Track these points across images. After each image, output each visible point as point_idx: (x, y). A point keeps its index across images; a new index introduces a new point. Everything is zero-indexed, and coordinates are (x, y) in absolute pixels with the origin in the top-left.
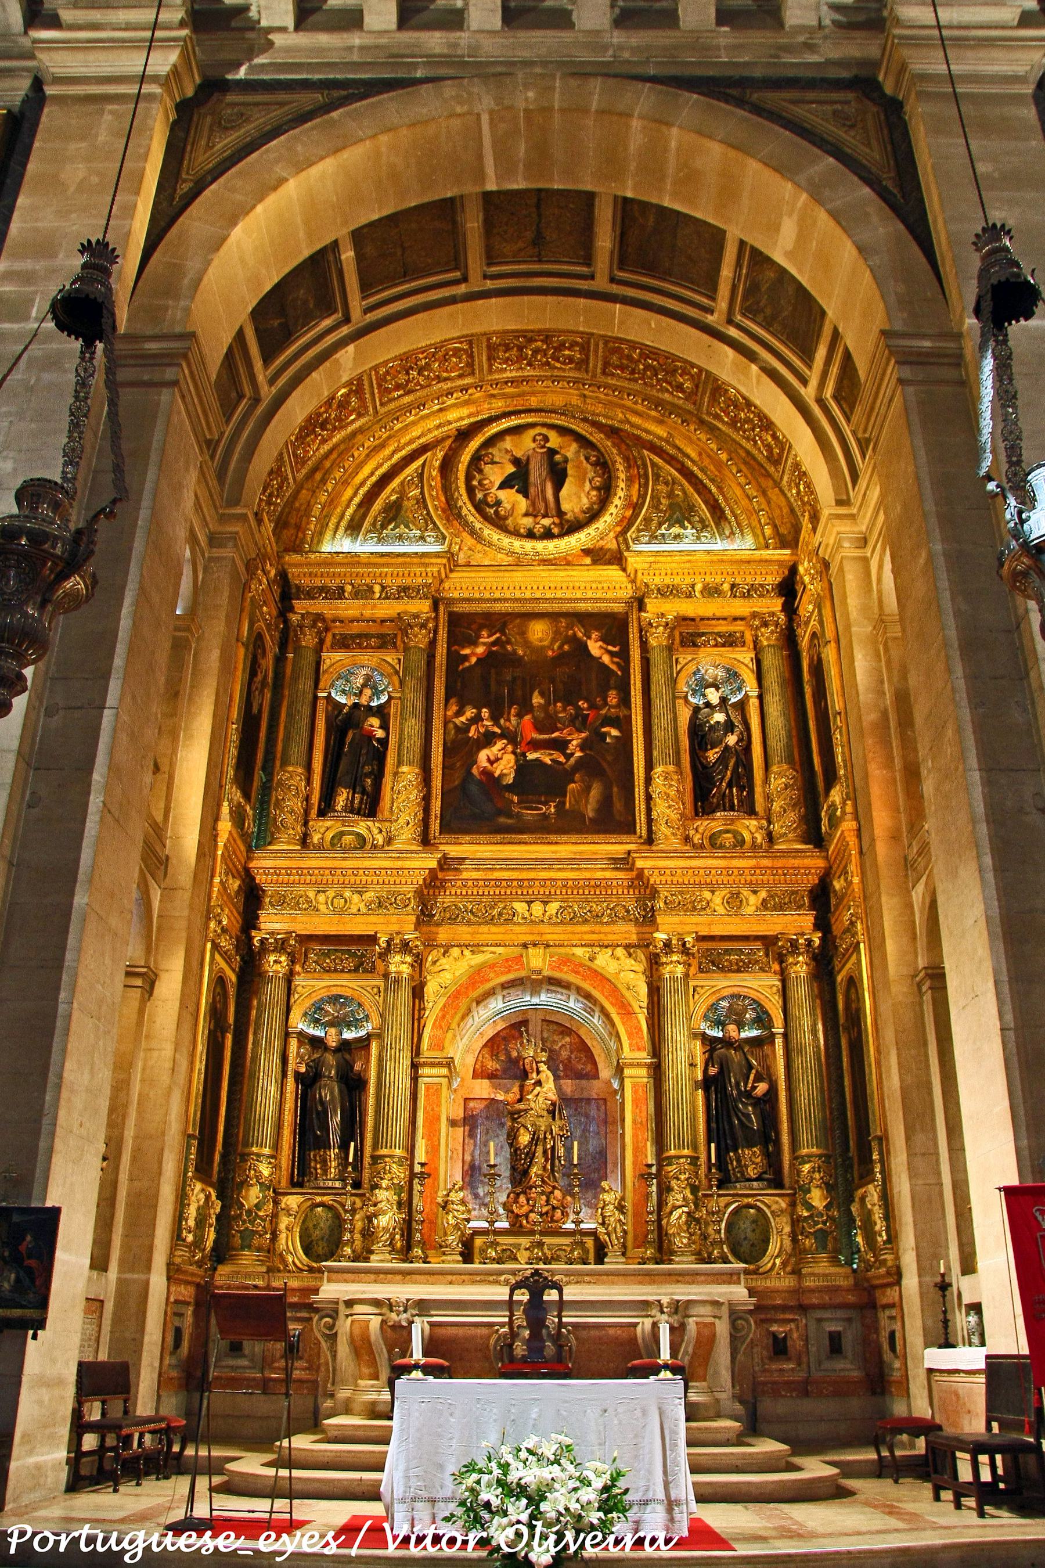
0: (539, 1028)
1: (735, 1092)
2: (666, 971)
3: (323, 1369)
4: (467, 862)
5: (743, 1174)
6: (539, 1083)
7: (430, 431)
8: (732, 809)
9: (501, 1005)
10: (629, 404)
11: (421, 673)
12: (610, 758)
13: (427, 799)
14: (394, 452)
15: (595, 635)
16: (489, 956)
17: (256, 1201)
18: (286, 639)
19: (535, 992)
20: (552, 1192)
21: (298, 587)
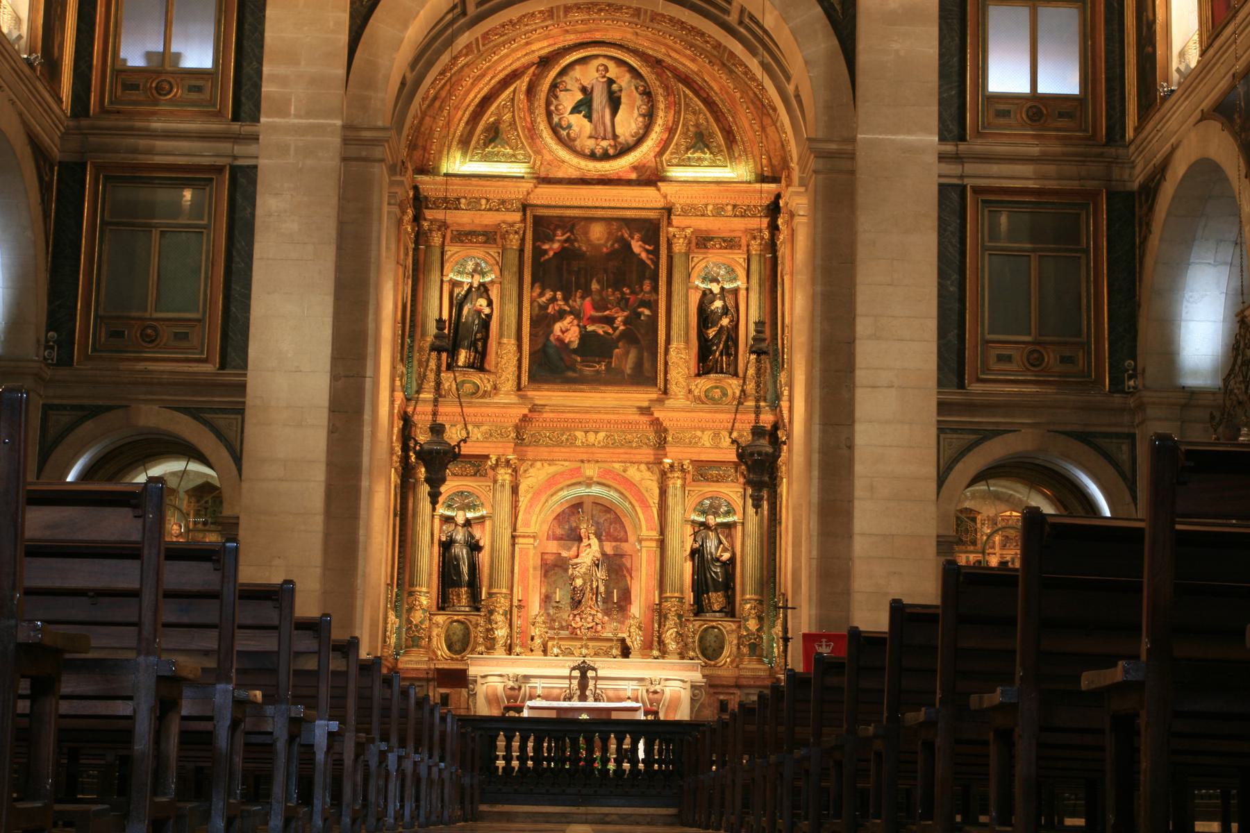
5: (711, 607)
7: (519, 59)
8: (722, 372)
10: (671, 43)
11: (515, 269)
12: (643, 331)
13: (520, 361)
14: (491, 80)
15: (637, 236)
18: (420, 237)
21: (426, 198)
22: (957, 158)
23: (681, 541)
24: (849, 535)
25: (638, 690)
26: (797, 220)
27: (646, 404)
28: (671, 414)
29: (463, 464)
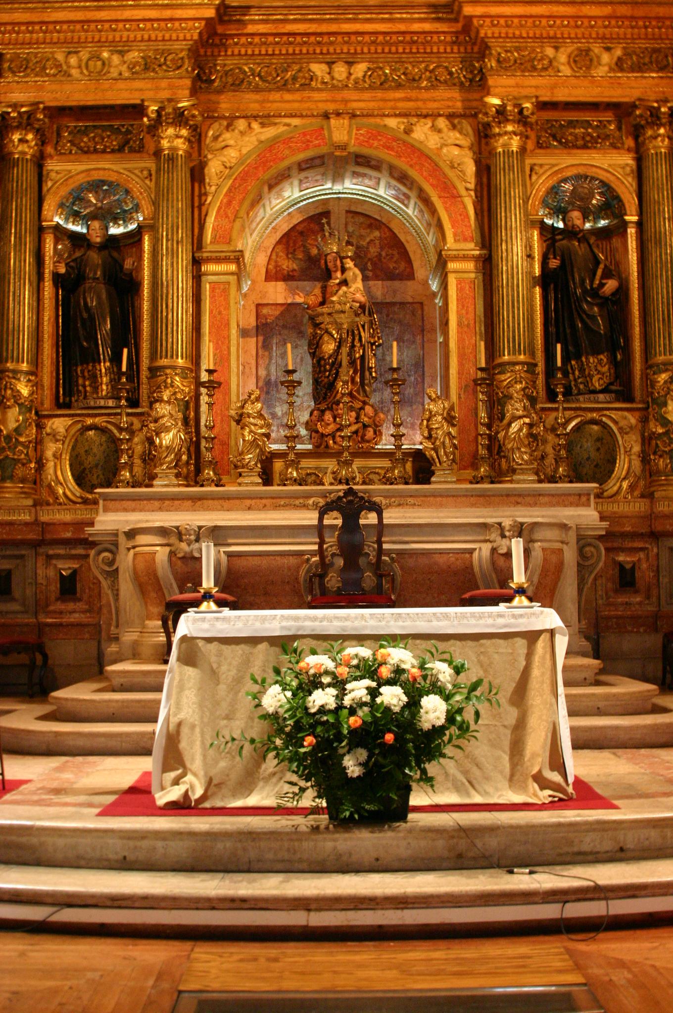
0: (343, 221)
1: (579, 291)
2: (499, 146)
3: (105, 610)
4: (253, 11)
5: (586, 384)
9: (297, 194)
16: (282, 129)
17: (15, 425)
19: (338, 177)
20: (362, 408)
25: (471, 551)
29: (99, 131)
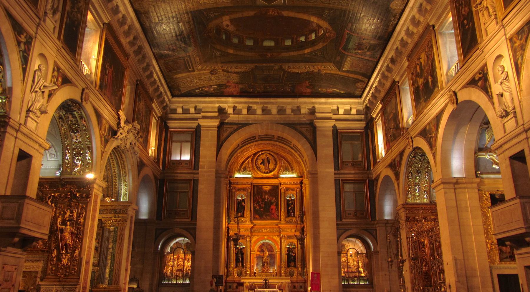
6: (266, 253)
11: (250, 196)
13: (251, 215)
22: (338, 174)
23: (284, 251)
24: (319, 252)
26: (306, 186)
27: (277, 223)
28: (282, 226)
